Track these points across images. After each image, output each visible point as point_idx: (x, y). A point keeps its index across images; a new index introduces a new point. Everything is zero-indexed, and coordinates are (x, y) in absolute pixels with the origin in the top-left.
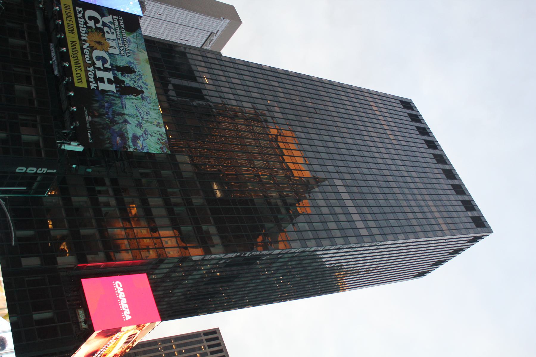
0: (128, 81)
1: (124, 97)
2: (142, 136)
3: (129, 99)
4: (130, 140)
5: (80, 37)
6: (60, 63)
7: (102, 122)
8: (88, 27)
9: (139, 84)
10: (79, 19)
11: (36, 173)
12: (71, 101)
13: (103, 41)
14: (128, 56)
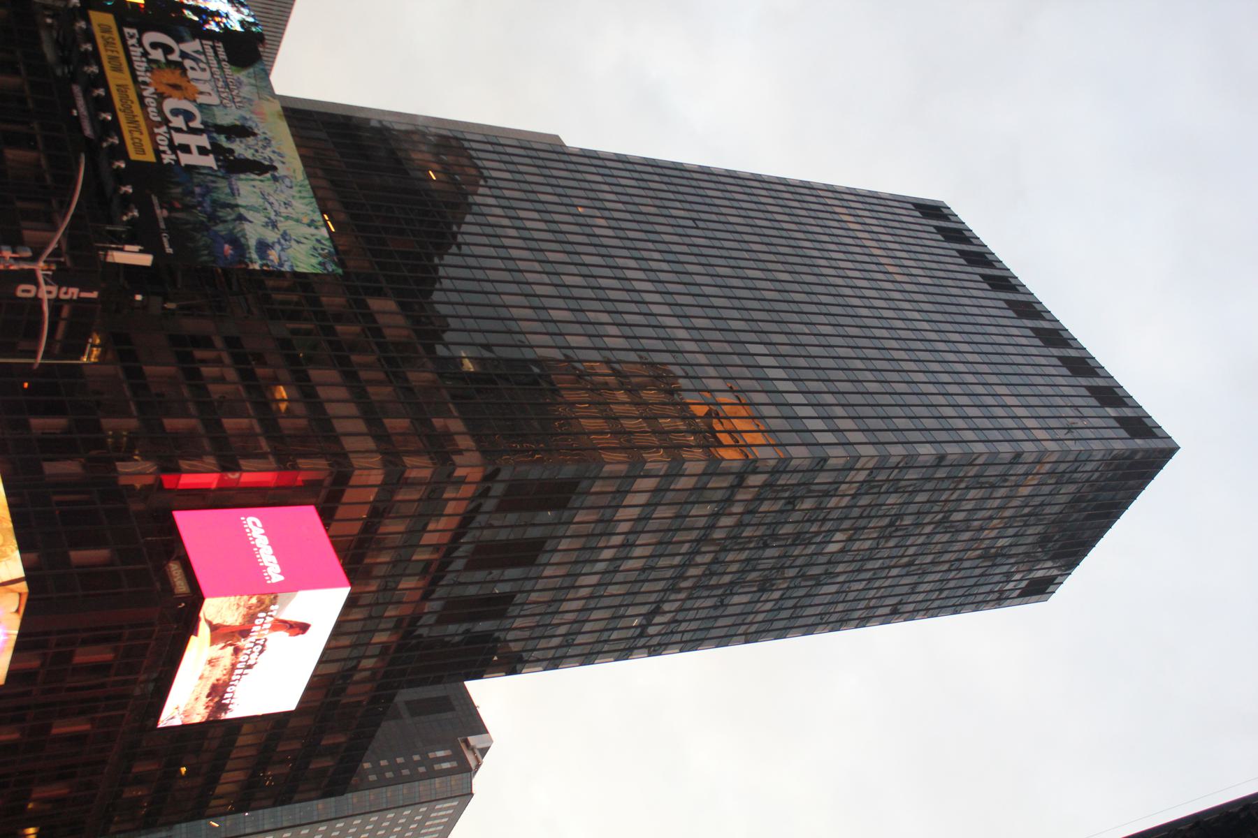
0: (241, 149)
1: (234, 177)
2: (279, 242)
5: (134, 77)
6: (93, 117)
8: (150, 61)
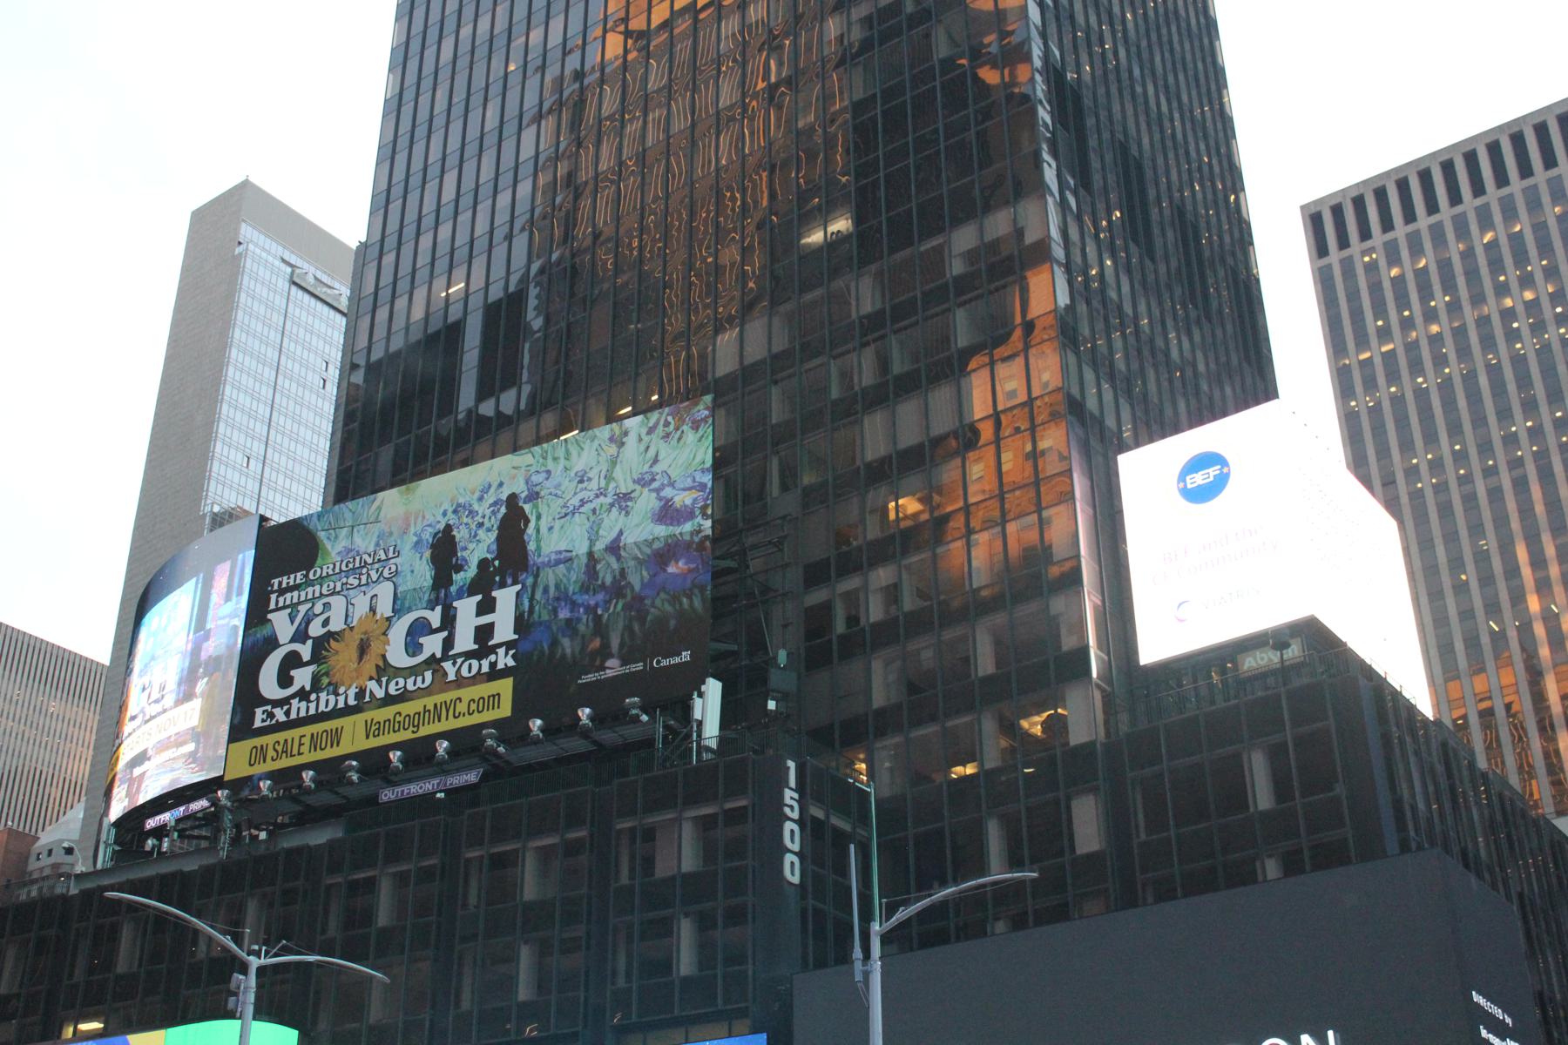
0: (478, 548)
2: (657, 491)
3: (538, 540)
4: (677, 530)
5: (348, 711)
6: (442, 769)
7: (621, 625)
9: (488, 512)
10: (293, 716)
11: (801, 822)
13: (357, 636)
14: (397, 554)
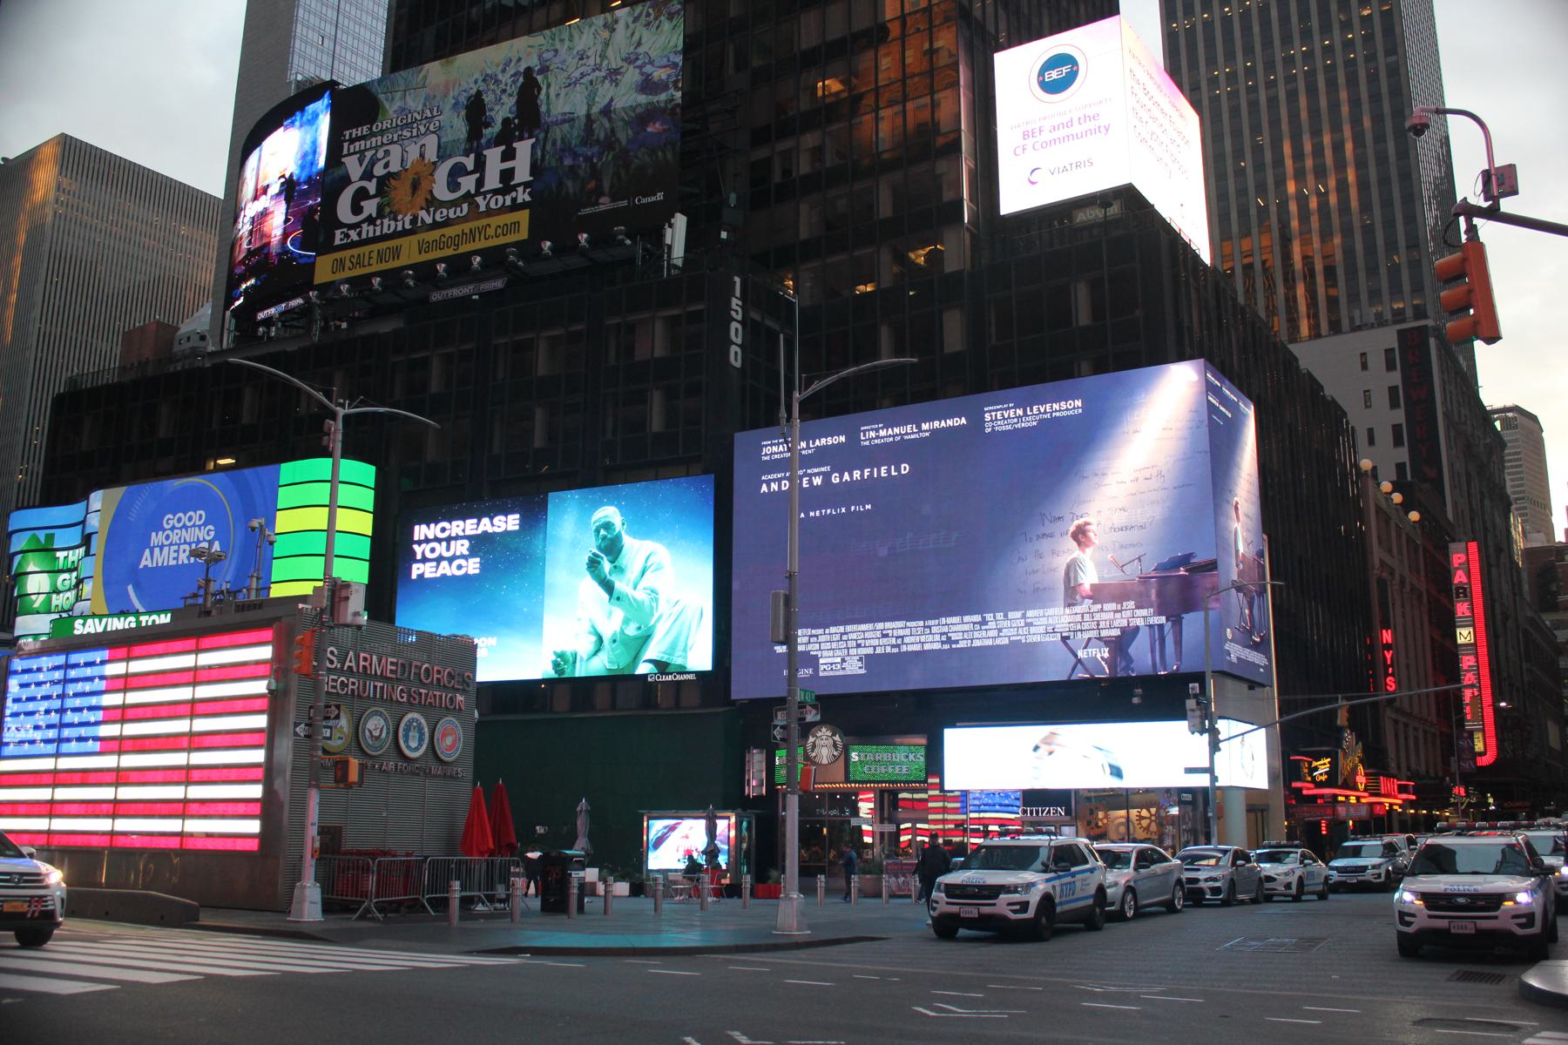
0: (502, 110)
1: (545, 119)
2: (640, 67)
3: (548, 104)
4: (655, 99)
5: (405, 233)
6: (477, 277)
8: (381, 214)
10: (364, 236)
11: (742, 323)
12: (565, 247)
13: (411, 177)
